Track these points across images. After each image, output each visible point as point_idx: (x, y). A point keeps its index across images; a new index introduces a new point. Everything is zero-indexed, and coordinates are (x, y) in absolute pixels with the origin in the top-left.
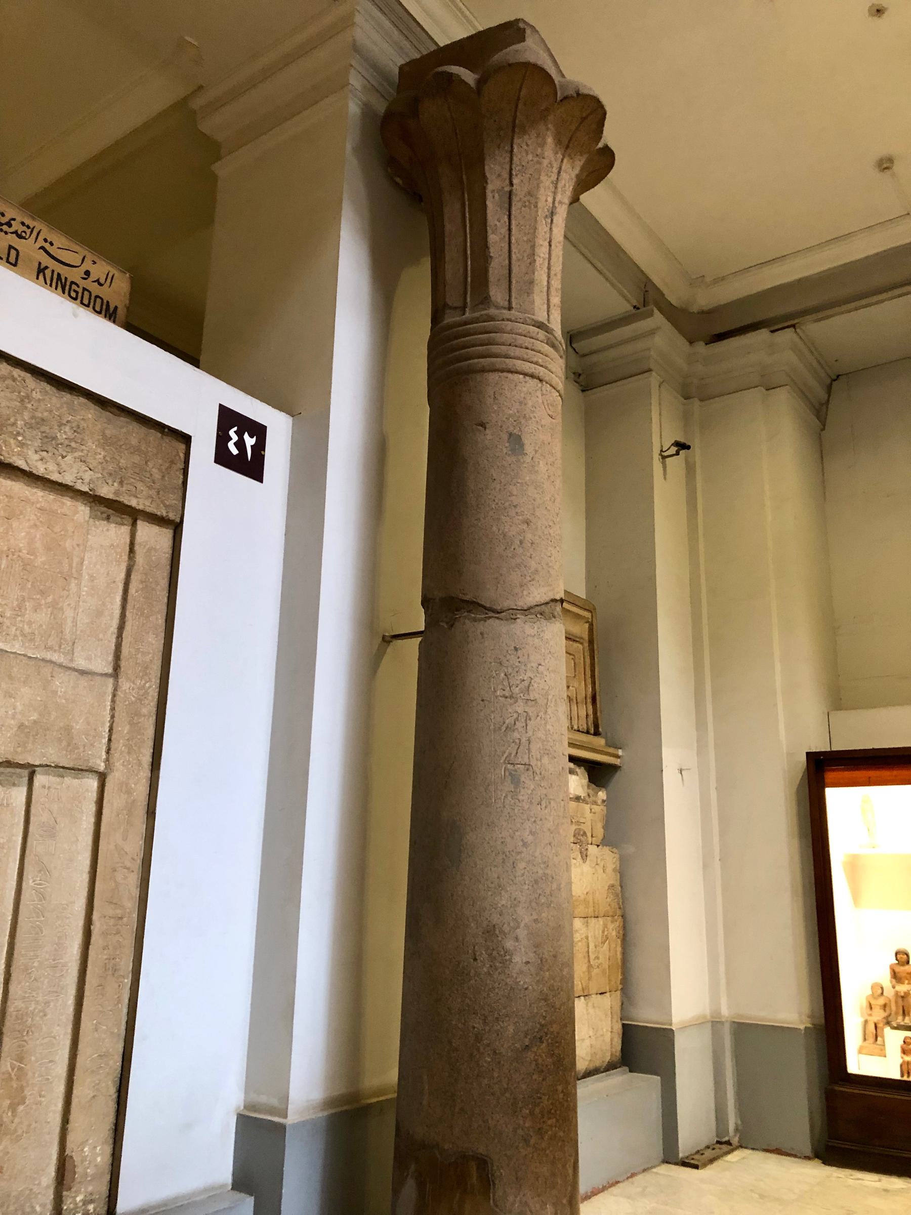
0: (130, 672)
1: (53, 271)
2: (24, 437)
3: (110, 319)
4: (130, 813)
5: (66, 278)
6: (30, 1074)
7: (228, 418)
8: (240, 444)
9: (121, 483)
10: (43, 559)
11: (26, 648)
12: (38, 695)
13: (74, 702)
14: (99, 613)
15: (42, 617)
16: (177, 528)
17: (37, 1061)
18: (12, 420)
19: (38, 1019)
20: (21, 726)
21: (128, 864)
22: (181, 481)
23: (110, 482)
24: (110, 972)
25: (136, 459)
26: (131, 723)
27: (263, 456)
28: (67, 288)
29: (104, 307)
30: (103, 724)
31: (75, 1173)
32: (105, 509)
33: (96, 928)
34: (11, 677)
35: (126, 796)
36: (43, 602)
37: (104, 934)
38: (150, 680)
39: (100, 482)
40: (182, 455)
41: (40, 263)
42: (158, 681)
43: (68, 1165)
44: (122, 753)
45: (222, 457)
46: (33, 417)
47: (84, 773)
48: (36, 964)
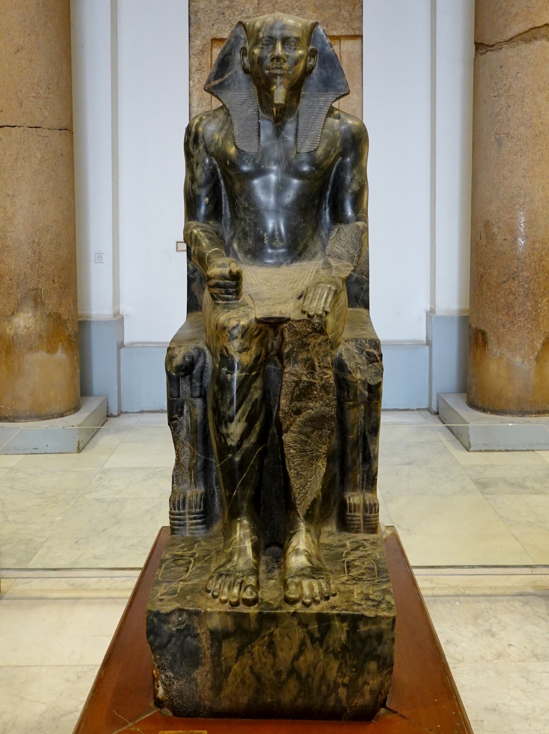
25: (334, 11)
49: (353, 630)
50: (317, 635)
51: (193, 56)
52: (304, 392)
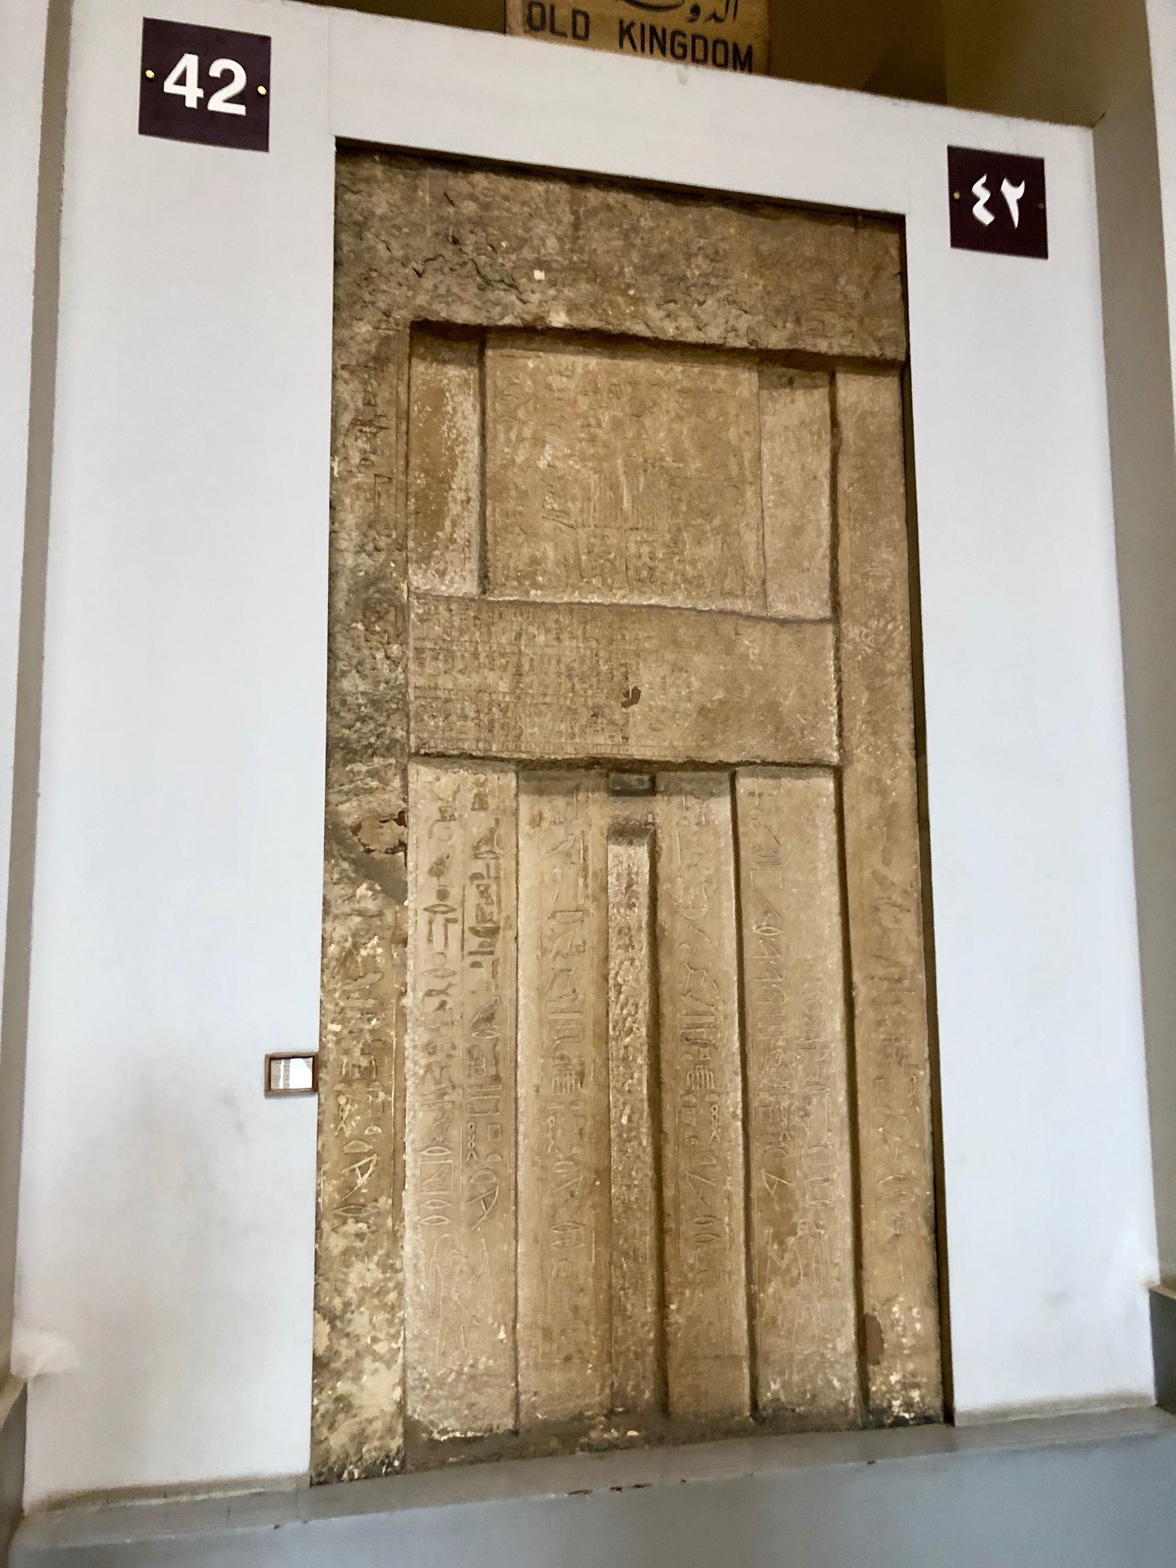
0: (857, 611)
1: (643, 27)
2: (638, 289)
3: (742, 70)
4: (890, 823)
5: (664, 31)
6: (798, 1194)
7: (965, 165)
8: (997, 204)
9: (798, 321)
10: (698, 464)
11: (693, 599)
12: (720, 664)
13: (775, 666)
14: (798, 531)
15: (710, 550)
16: (902, 369)
17: (806, 1176)
18: (616, 269)
19: (797, 1119)
20: (703, 711)
21: (900, 900)
22: (898, 295)
23: (780, 324)
24: (894, 1059)
25: (817, 277)
26: (870, 688)
27: (1044, 211)
28: (668, 45)
29: (731, 55)
30: (827, 696)
31: (882, 1341)
32: (784, 370)
33: (861, 993)
34: (676, 643)
35: (879, 798)
36: (708, 527)
37: (874, 1003)
38: (894, 619)
39: (763, 328)
40: (894, 252)
41: (621, 22)
42: (908, 618)
43: (870, 1328)
44: (862, 734)
45: (965, 234)
46: (644, 257)
47: (810, 770)
48: (781, 1043)
51: (345, 374)
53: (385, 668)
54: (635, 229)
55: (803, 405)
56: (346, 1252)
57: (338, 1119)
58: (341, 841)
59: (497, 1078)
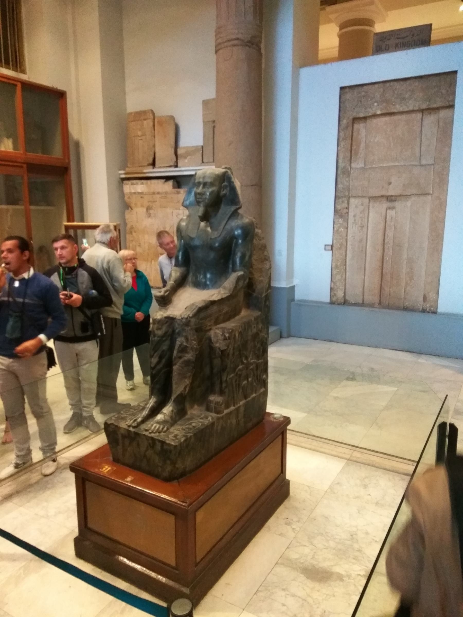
9: (430, 102)
49: (162, 447)
50: (151, 445)
52: (183, 350)
53: (345, 183)
54: (396, 89)
55: (430, 119)
56: (336, 274)
57: (335, 254)
58: (337, 212)
59: (362, 250)
